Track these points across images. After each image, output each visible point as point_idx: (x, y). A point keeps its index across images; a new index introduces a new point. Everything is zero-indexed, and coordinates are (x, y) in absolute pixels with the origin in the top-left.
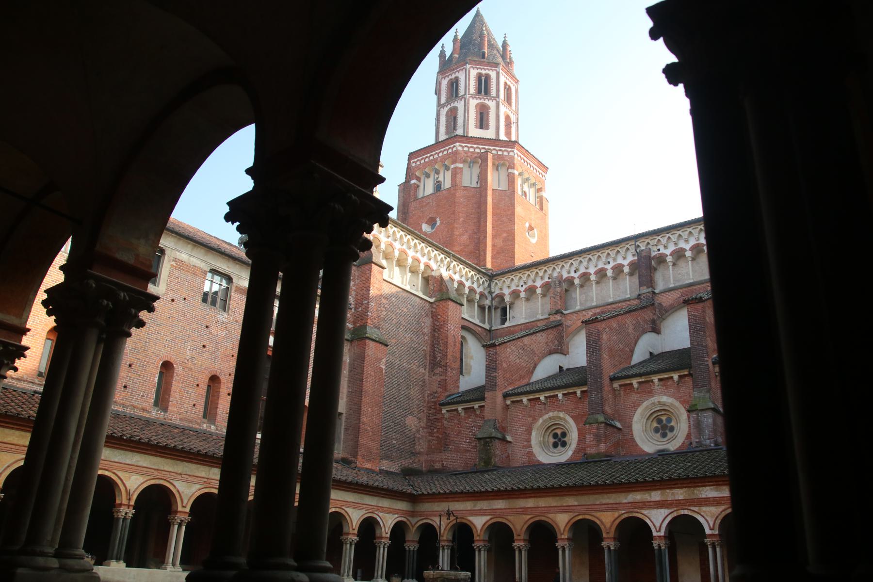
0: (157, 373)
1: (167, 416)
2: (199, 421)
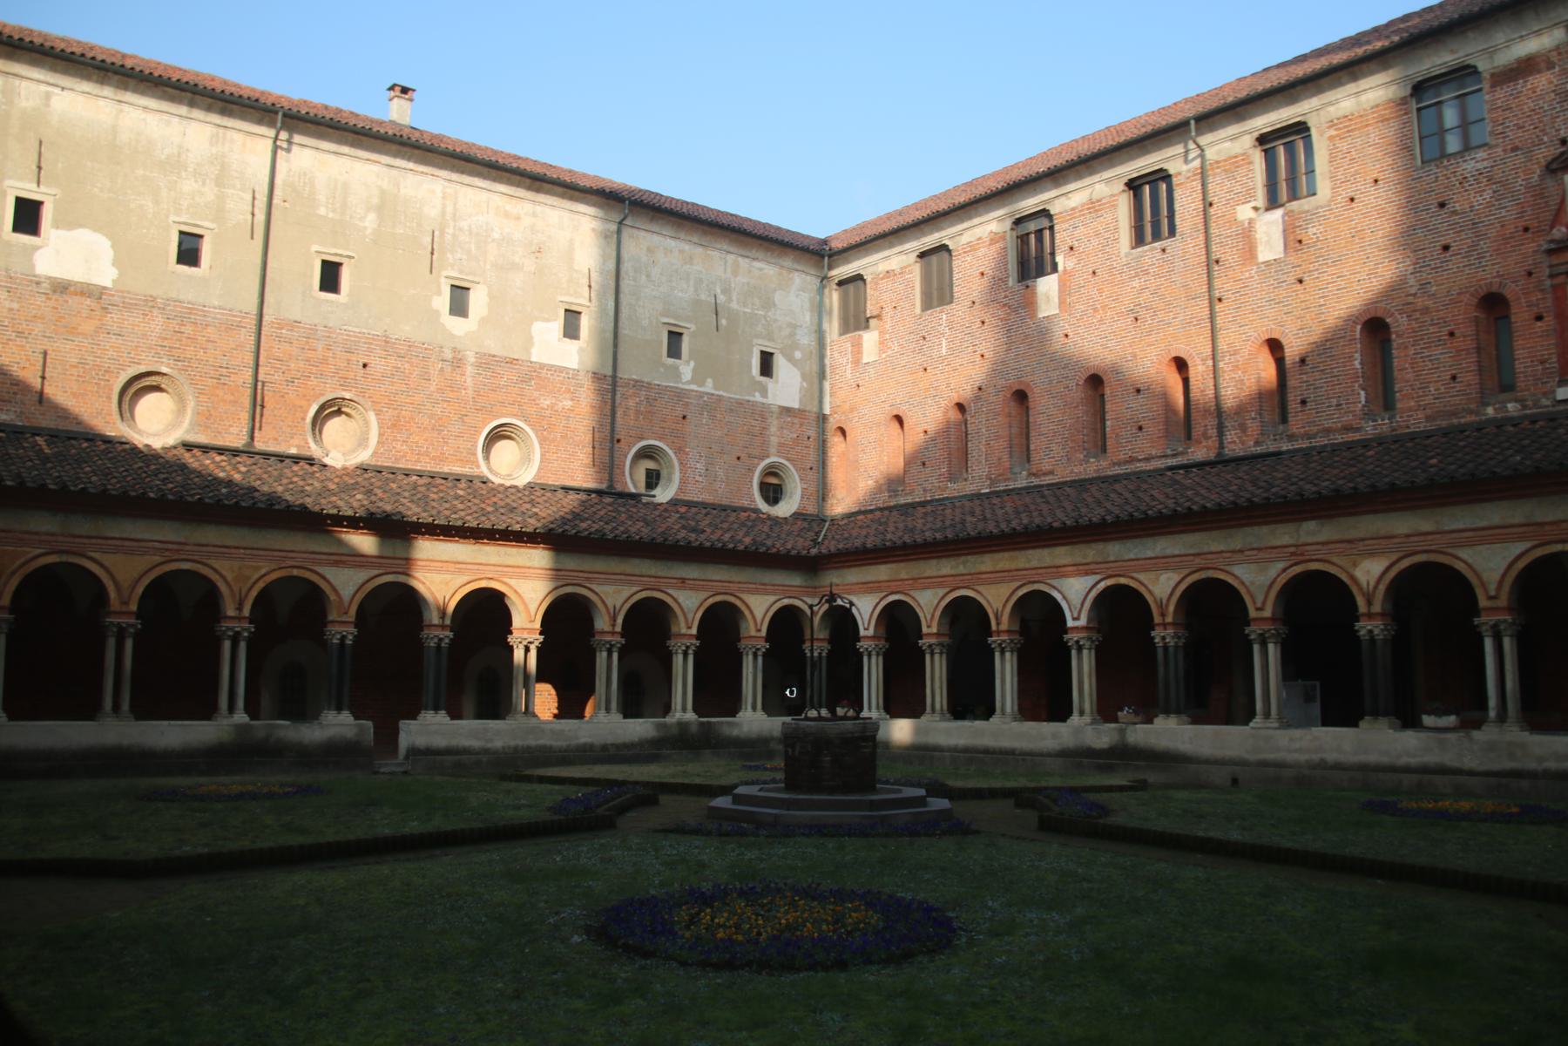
0: (1356, 352)
1: (1397, 422)
2: (1473, 406)
